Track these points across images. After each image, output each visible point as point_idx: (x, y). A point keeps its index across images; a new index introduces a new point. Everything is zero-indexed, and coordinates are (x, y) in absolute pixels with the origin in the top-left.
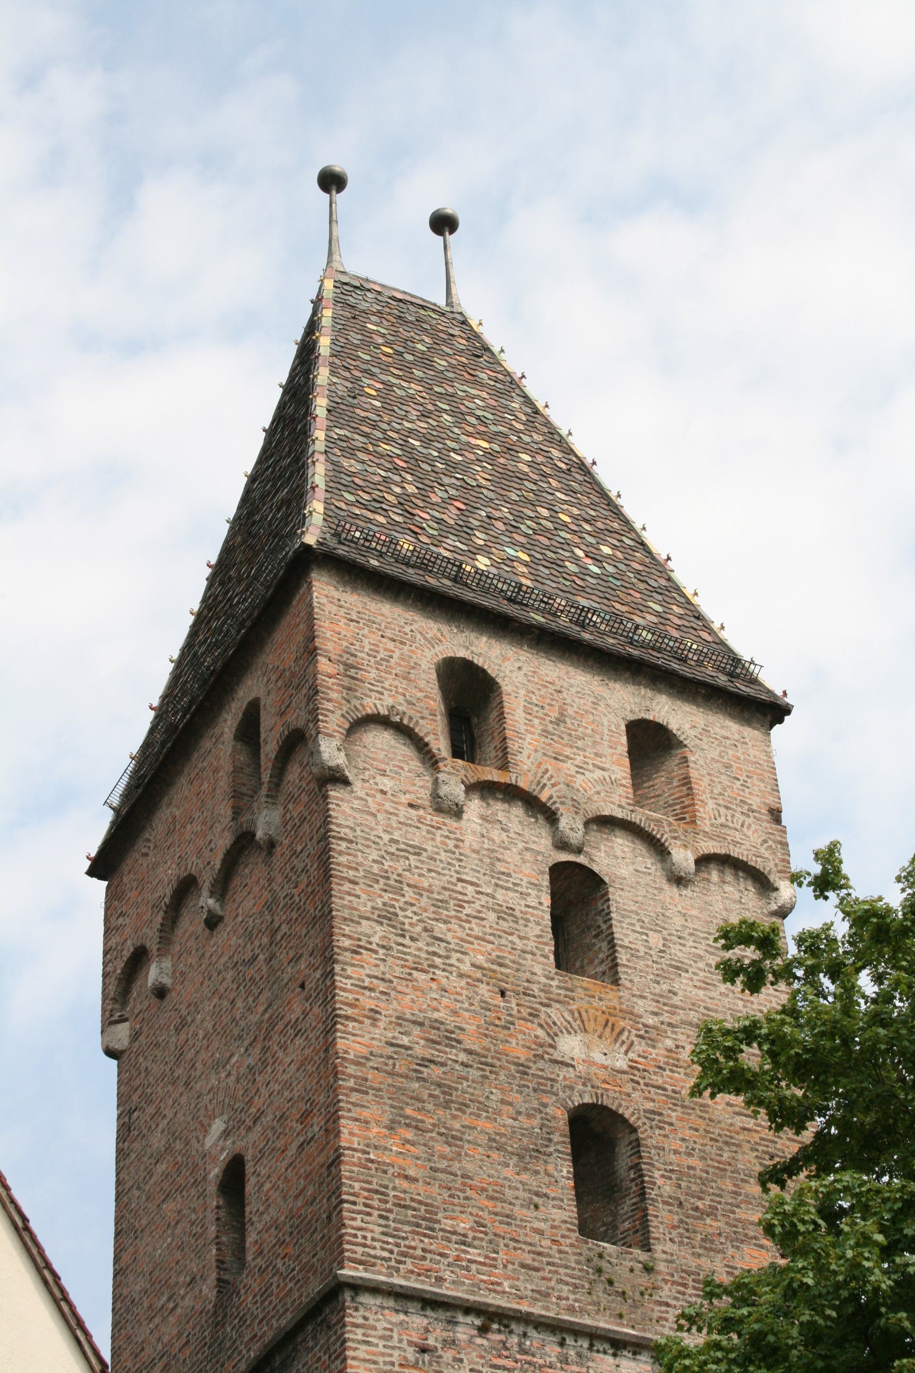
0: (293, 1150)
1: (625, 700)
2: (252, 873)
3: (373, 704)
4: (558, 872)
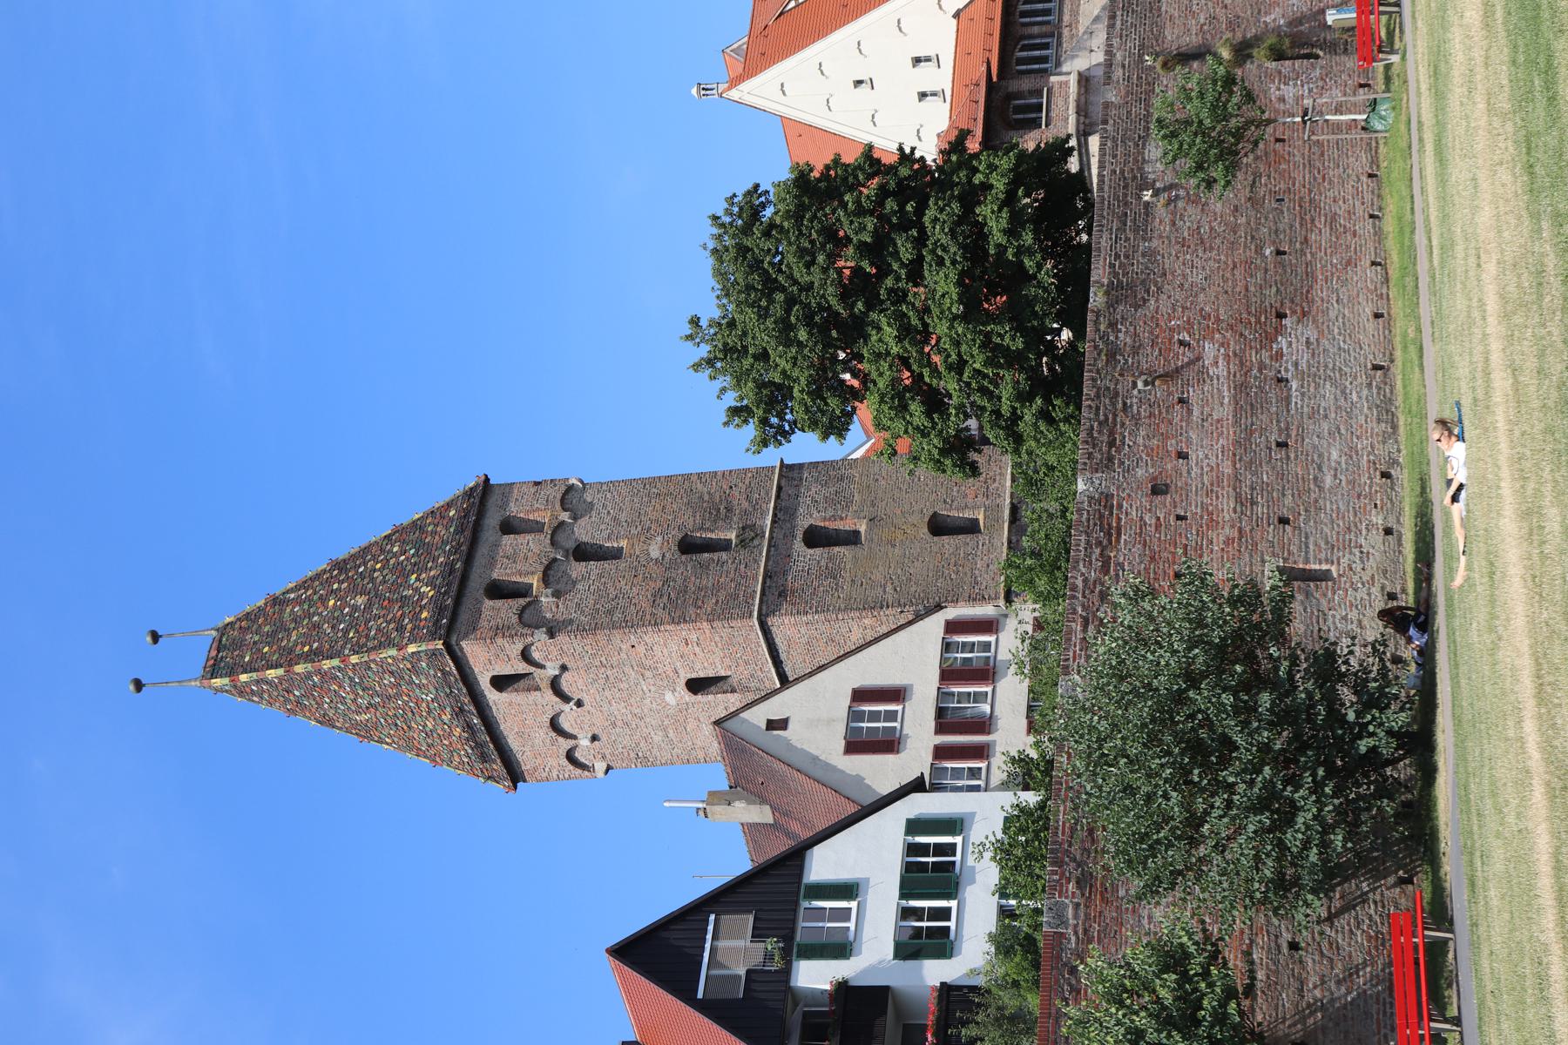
0: (697, 649)
2: (565, 685)
3: (515, 619)
4: (577, 559)
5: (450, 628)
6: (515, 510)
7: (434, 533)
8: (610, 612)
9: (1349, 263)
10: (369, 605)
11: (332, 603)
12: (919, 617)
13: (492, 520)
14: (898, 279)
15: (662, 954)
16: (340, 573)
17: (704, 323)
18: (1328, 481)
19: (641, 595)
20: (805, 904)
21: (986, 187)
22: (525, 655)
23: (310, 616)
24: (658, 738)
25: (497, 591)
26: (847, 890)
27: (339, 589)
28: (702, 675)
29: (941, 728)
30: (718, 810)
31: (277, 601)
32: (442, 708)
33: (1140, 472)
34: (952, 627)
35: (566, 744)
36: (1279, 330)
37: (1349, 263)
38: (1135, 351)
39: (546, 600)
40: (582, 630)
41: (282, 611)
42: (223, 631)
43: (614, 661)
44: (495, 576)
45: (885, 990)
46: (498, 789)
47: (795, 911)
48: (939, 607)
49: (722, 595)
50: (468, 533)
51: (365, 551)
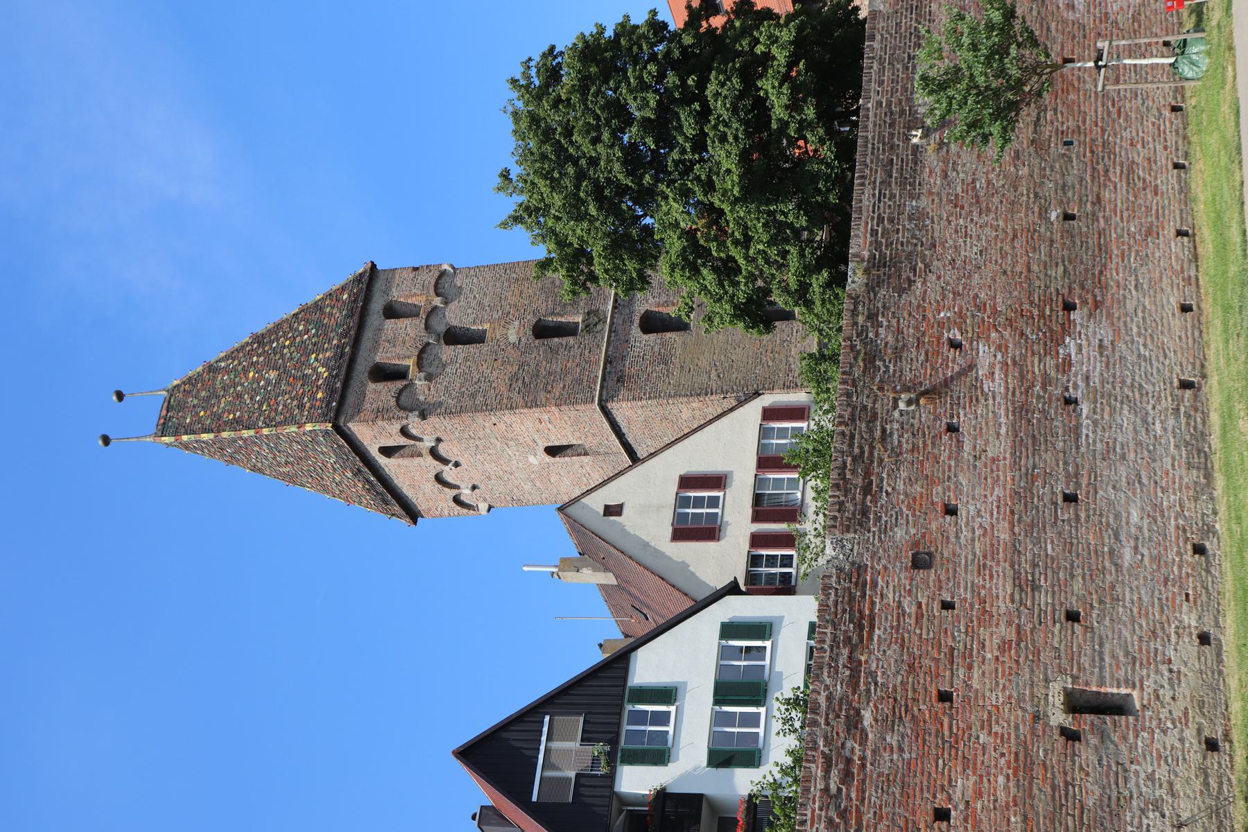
0: (550, 426)
1: (375, 317)
2: (443, 450)
3: (393, 402)
4: (448, 343)
5: (337, 417)
6: (398, 295)
7: (331, 314)
8: (473, 396)
9: (1149, 233)
10: (279, 381)
11: (251, 374)
12: (741, 403)
13: (377, 305)
14: (683, 152)
15: (498, 755)
16: (258, 347)
17: (513, 176)
18: (1127, 556)
19: (499, 378)
20: (629, 707)
21: (767, 57)
22: (404, 432)
23: (235, 385)
24: (528, 487)
25: (383, 374)
26: (666, 694)
27: (257, 362)
28: (557, 444)
29: (757, 517)
30: (570, 577)
31: (212, 369)
33: (899, 533)
34: (770, 414)
36: (1067, 328)
37: (1149, 233)
38: (898, 354)
39: (420, 383)
40: (449, 413)
41: (215, 378)
42: (172, 391)
43: (481, 434)
44: (378, 359)
45: (698, 798)
46: (403, 523)
47: (620, 714)
48: (757, 394)
49: (568, 380)
50: (356, 318)
51: (278, 326)
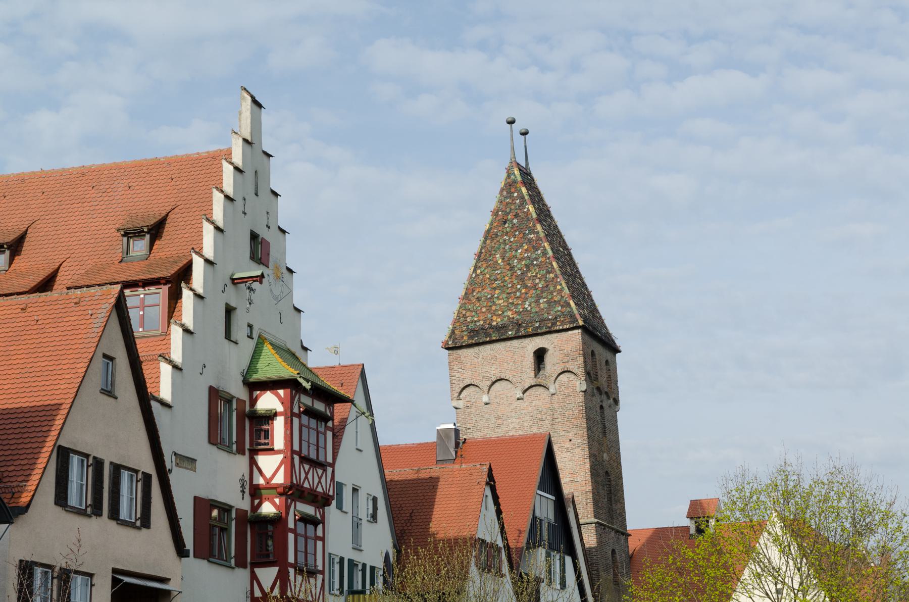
32: (519, 313)
35: (485, 384)
